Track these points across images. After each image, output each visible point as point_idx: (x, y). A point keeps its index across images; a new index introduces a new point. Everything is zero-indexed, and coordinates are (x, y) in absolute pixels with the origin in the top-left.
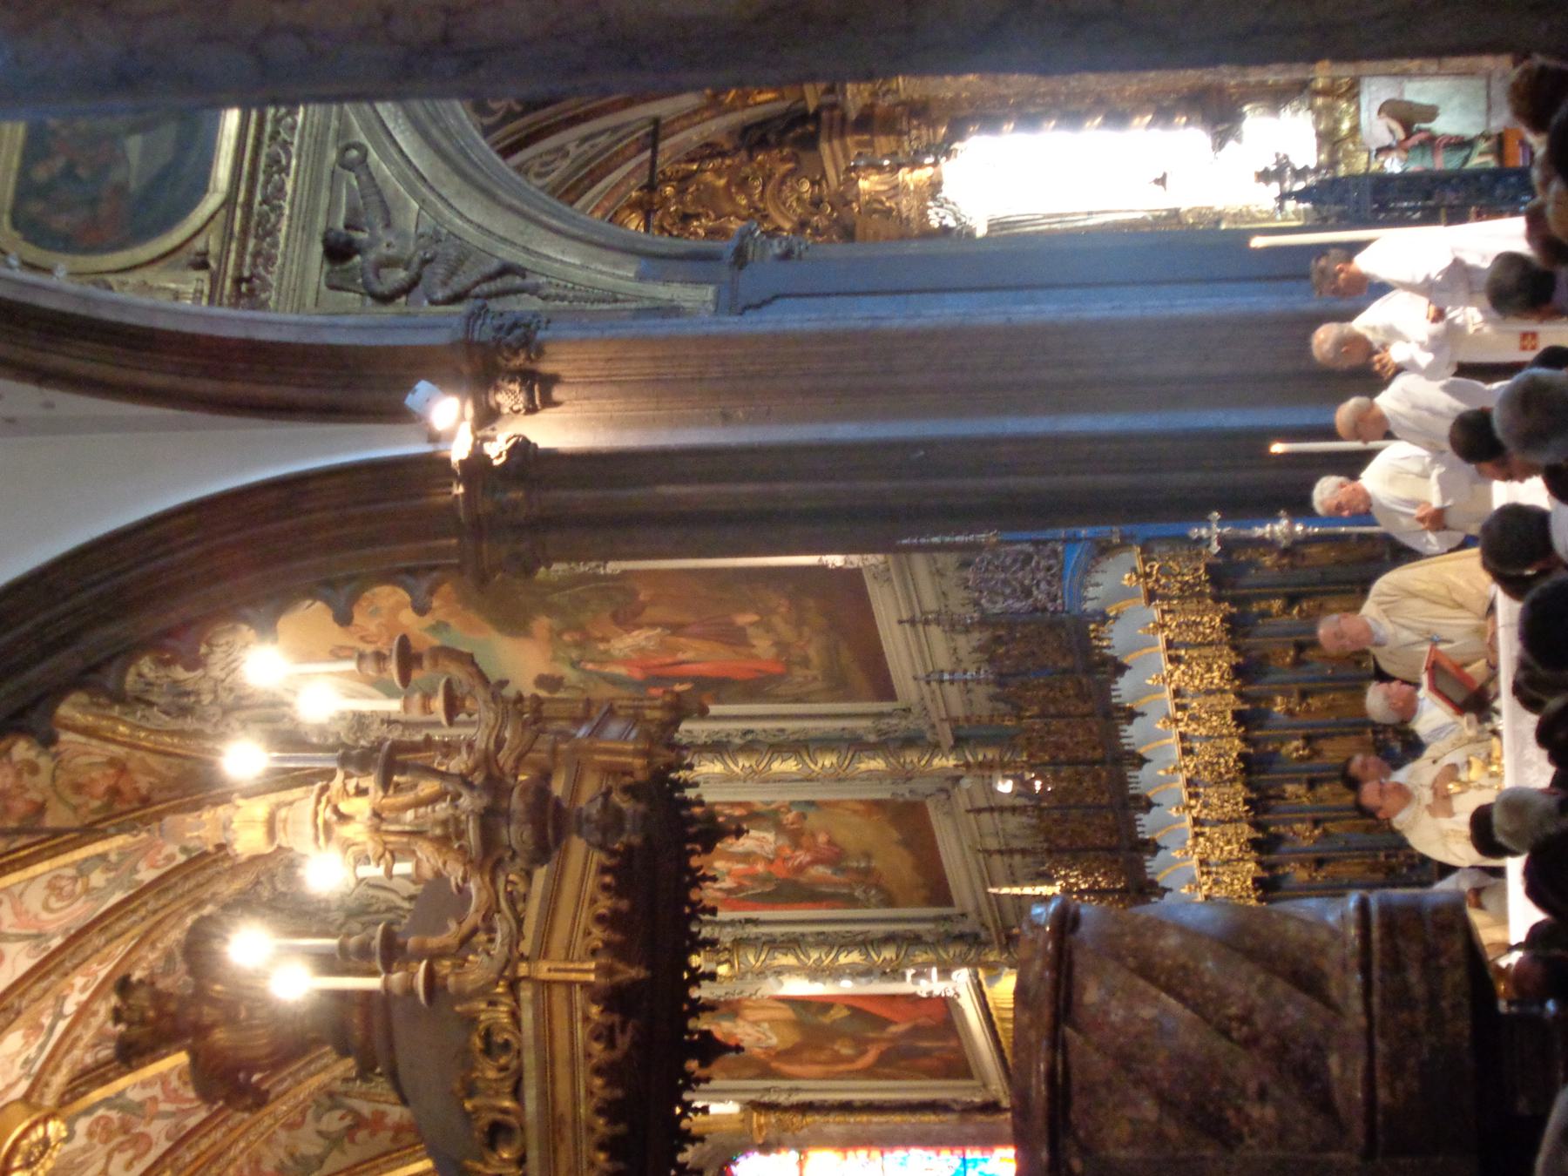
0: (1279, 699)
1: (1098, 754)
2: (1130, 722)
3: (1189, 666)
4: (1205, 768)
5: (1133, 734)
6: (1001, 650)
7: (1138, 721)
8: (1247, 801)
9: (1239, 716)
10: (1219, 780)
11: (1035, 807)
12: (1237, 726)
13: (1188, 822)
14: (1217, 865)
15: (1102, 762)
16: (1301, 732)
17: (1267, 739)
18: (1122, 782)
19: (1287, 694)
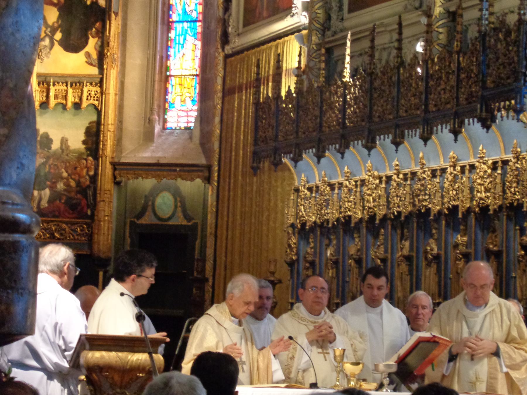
0: (465, 239)
1: (432, 108)
2: (451, 131)
3: (490, 176)
4: (422, 185)
5: (444, 133)
6: (501, 36)
7: (452, 136)
8: (399, 213)
9: (456, 208)
10: (414, 195)
11: (402, 64)
12: (448, 209)
13: (389, 173)
14: (361, 192)
15: (426, 111)
16: (442, 253)
17: (439, 229)
18: (412, 126)
19: (467, 245)
